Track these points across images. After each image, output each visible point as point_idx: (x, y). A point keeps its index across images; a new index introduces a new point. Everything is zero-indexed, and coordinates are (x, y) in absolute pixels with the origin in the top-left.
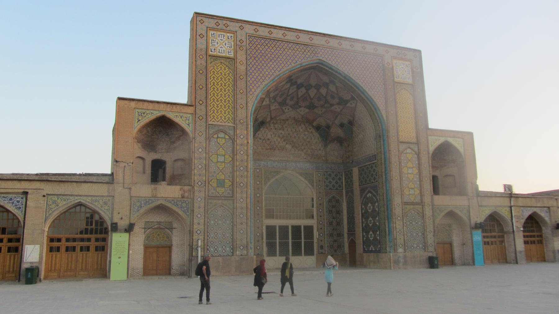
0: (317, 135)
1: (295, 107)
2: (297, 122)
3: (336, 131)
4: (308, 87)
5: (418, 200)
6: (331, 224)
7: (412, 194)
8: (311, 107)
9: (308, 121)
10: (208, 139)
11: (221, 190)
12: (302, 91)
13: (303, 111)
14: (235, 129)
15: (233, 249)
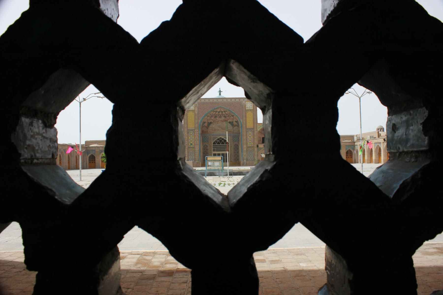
0: (230, 124)
1: (220, 117)
2: (222, 121)
3: (235, 123)
4: (222, 112)
5: (252, 146)
6: (235, 152)
7: (250, 144)
8: (225, 117)
9: (226, 121)
10: (188, 133)
11: (192, 146)
12: (220, 113)
13: (223, 118)
14: (195, 130)
15: (195, 161)
